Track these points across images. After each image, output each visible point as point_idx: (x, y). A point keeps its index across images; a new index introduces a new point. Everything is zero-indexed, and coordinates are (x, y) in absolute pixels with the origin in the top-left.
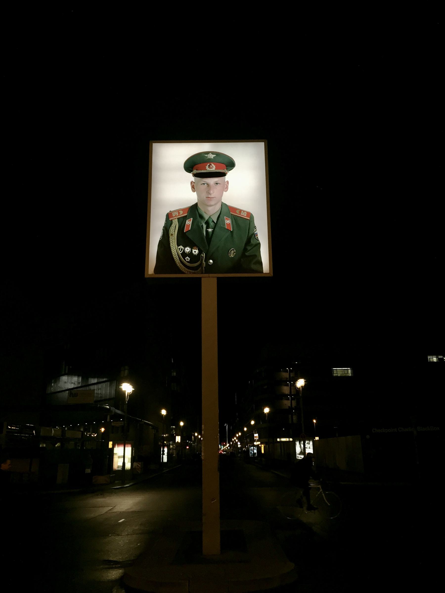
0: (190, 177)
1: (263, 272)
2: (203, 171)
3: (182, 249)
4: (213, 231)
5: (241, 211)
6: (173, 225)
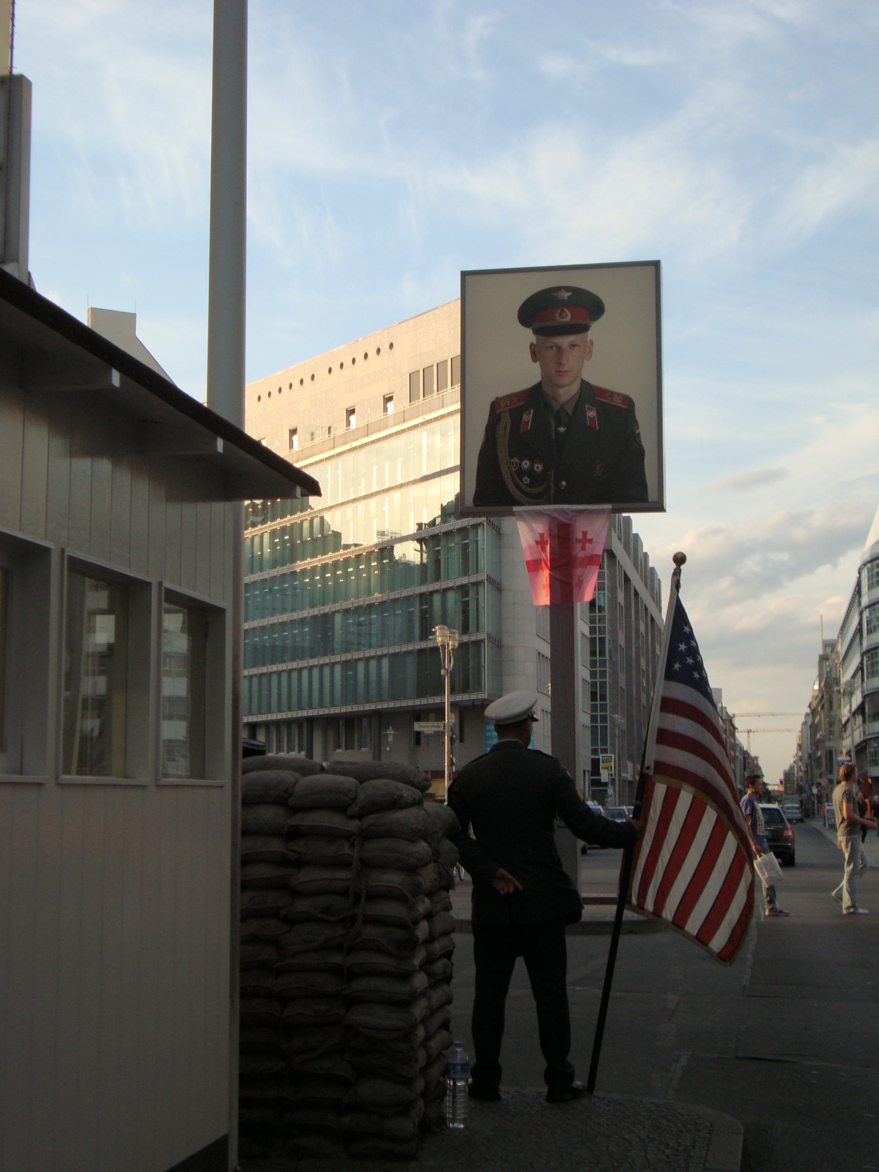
0: (528, 336)
5: (612, 394)
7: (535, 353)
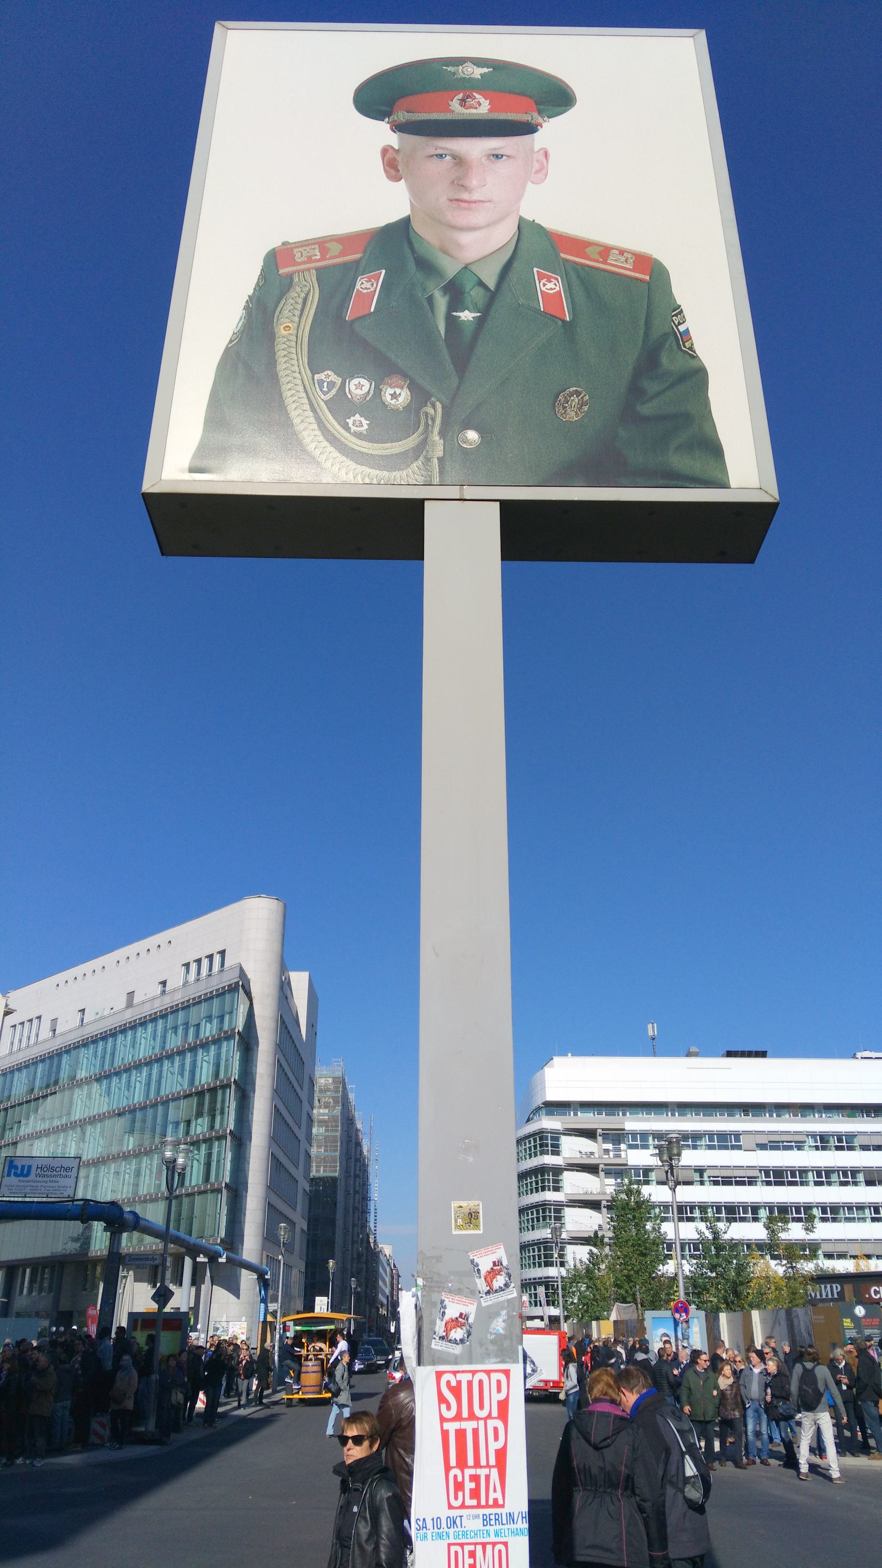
2: (434, 116)
3: (331, 385)
4: (480, 322)
5: (606, 251)
6: (295, 295)
7: (393, 165)
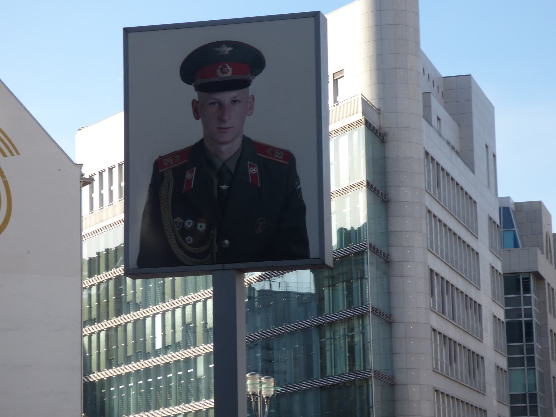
0: (190, 93)
1: (307, 257)
2: (212, 80)
3: (180, 223)
5: (274, 149)
7: (198, 110)
